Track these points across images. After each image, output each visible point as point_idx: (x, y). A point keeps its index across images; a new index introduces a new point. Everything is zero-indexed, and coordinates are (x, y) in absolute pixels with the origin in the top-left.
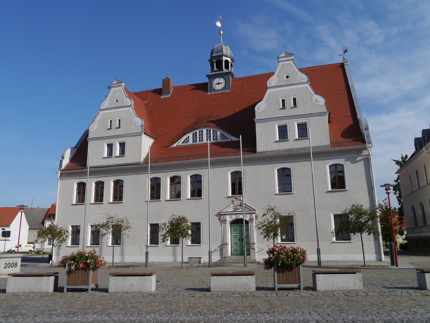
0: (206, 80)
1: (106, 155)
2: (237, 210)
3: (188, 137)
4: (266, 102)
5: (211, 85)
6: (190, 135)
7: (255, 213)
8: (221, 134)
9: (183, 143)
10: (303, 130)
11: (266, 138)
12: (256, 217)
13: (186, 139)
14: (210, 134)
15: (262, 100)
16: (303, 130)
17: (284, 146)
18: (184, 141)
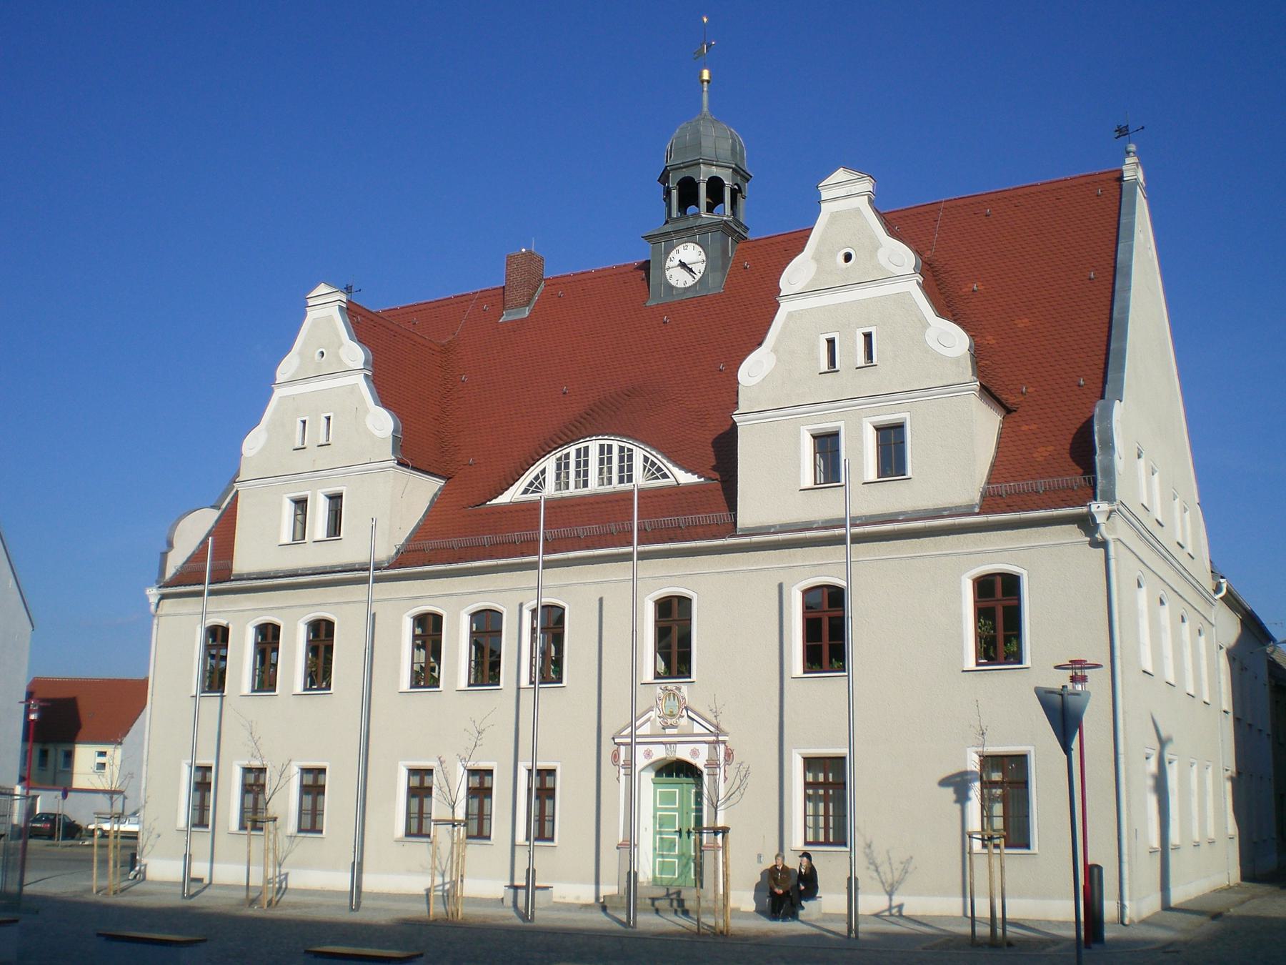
0: (644, 252)
1: (286, 537)
2: (668, 731)
3: (543, 472)
4: (775, 350)
5: (662, 269)
6: (549, 464)
7: (724, 742)
8: (646, 459)
9: (526, 491)
10: (892, 443)
11: (773, 479)
12: (729, 755)
13: (537, 478)
14: (610, 460)
15: (760, 344)
16: (892, 443)
17: (828, 505)
18: (531, 484)
